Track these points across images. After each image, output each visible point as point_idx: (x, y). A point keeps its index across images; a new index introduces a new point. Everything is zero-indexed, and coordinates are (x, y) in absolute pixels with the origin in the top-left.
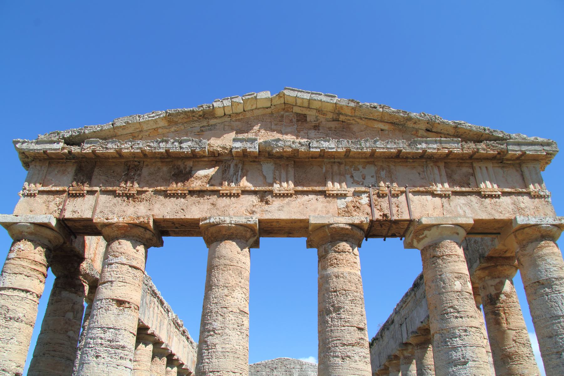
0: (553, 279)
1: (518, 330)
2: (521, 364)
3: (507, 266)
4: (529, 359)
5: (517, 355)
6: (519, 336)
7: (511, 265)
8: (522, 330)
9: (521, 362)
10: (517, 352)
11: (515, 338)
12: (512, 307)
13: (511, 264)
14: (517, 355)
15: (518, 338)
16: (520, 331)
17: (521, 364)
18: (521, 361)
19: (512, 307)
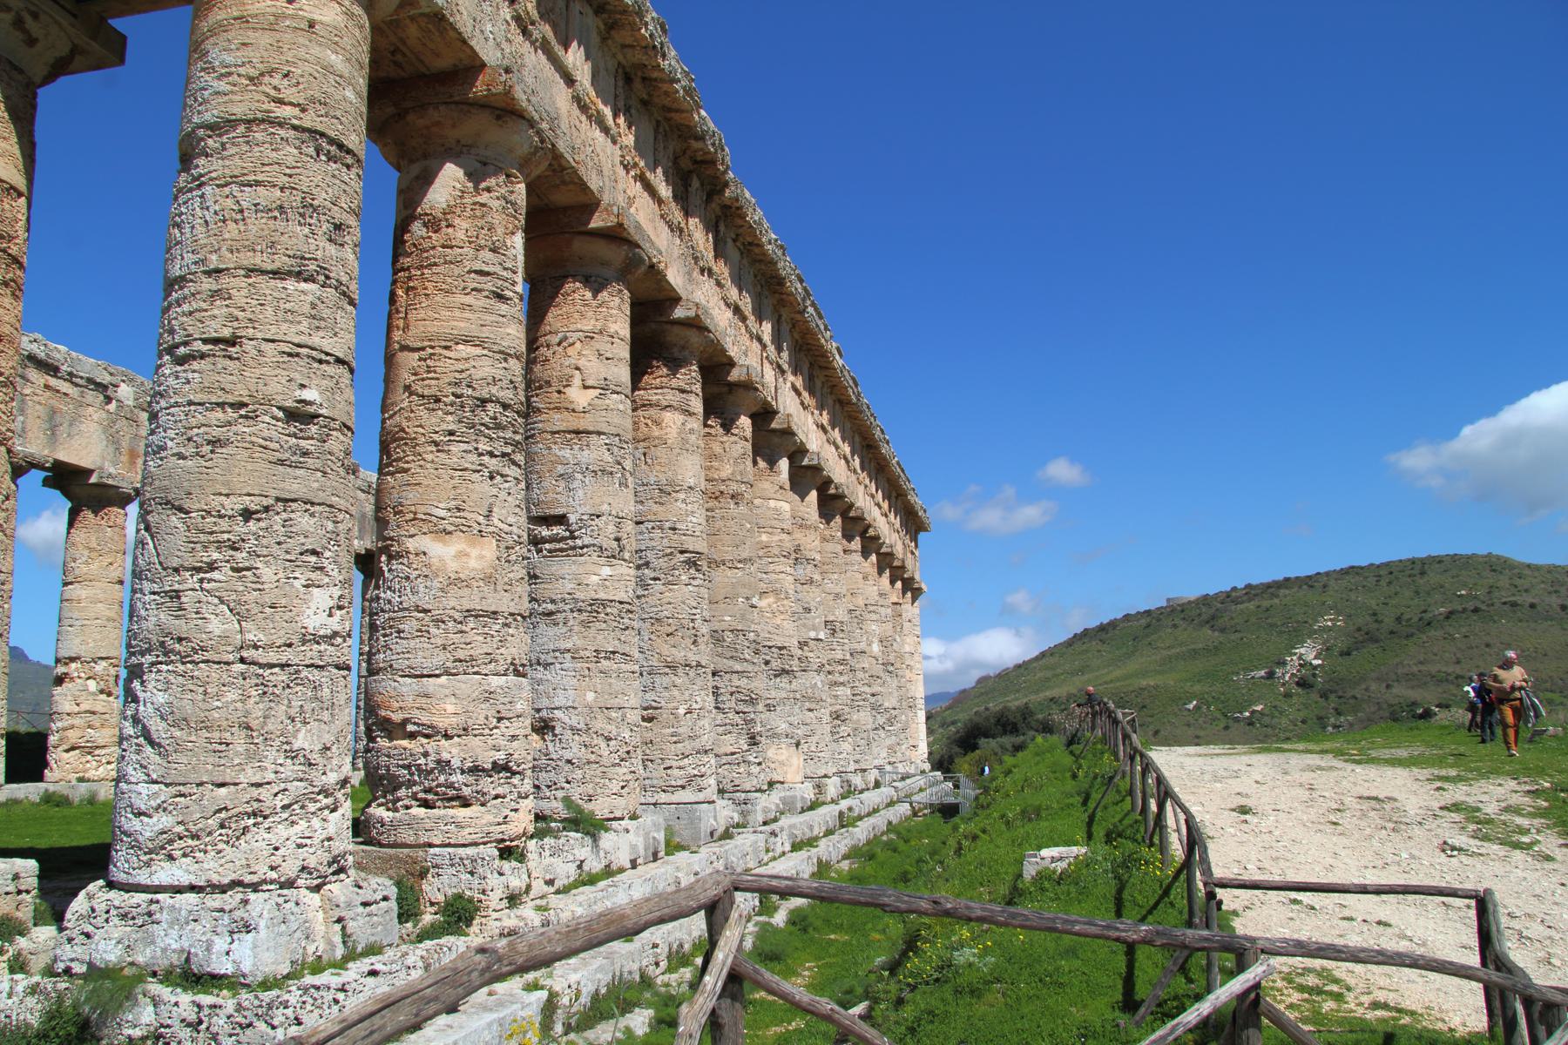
0: (201, 132)
1: (432, 347)
2: (406, 471)
3: (442, 108)
4: (438, 451)
5: (403, 439)
6: (429, 372)
7: (457, 103)
8: (446, 348)
9: (406, 466)
10: (403, 430)
11: (413, 378)
12: (435, 264)
13: (457, 98)
14: (403, 439)
15: (423, 380)
16: (438, 350)
17: (406, 471)
18: (408, 462)
19: (435, 264)
